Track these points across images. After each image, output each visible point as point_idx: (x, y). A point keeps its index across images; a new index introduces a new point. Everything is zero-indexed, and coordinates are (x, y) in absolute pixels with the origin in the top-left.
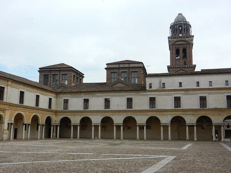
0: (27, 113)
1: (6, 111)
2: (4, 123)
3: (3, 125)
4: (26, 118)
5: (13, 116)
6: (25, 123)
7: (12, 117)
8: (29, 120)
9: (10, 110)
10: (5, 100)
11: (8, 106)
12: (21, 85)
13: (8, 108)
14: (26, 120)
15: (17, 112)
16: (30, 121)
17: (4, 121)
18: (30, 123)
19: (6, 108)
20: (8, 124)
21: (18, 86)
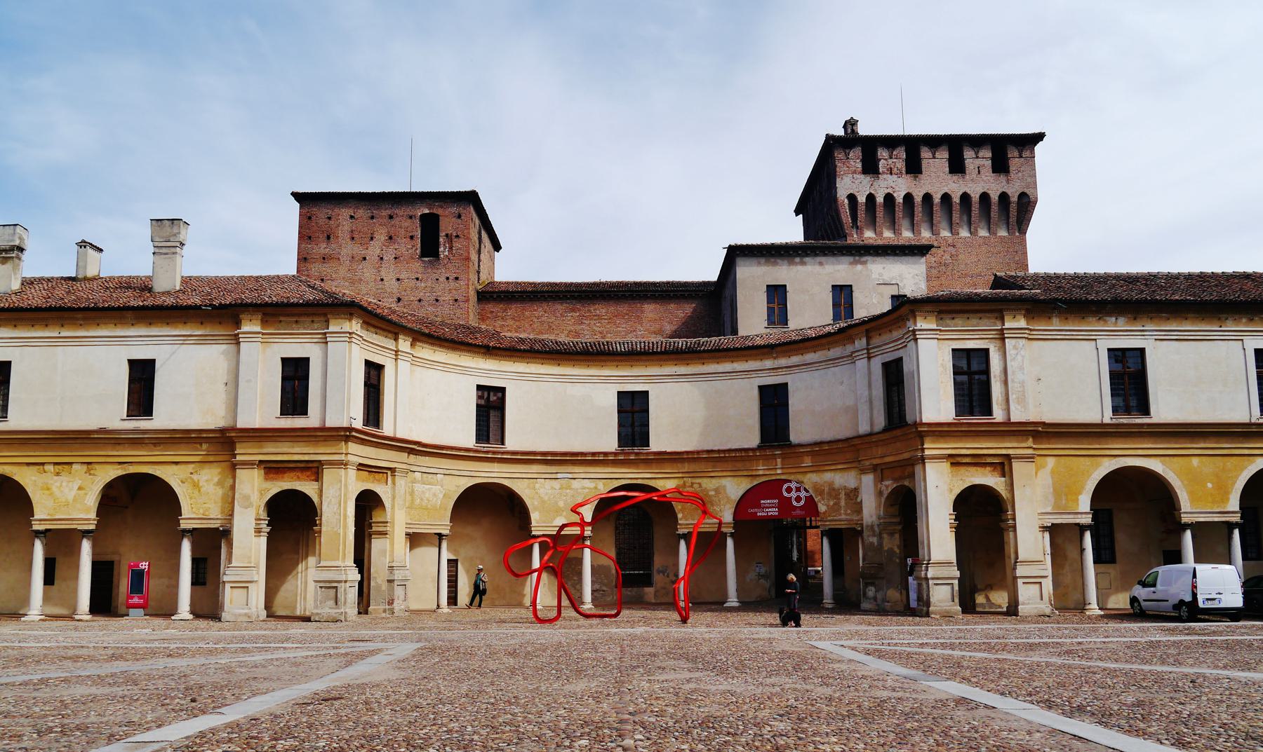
0: (1195, 461)
1: (1017, 466)
2: (1014, 527)
3: (1011, 534)
4: (1192, 494)
5: (1083, 488)
6: (1185, 519)
7: (1081, 494)
8: (1225, 499)
9: (1051, 462)
10: (998, 415)
11: (1030, 442)
12: (1110, 314)
13: (1030, 451)
14: (1193, 498)
15: (1107, 466)
16: (1234, 504)
17: (1014, 515)
18: (1236, 518)
19: (1010, 452)
20: (1054, 531)
21: (1092, 325)
